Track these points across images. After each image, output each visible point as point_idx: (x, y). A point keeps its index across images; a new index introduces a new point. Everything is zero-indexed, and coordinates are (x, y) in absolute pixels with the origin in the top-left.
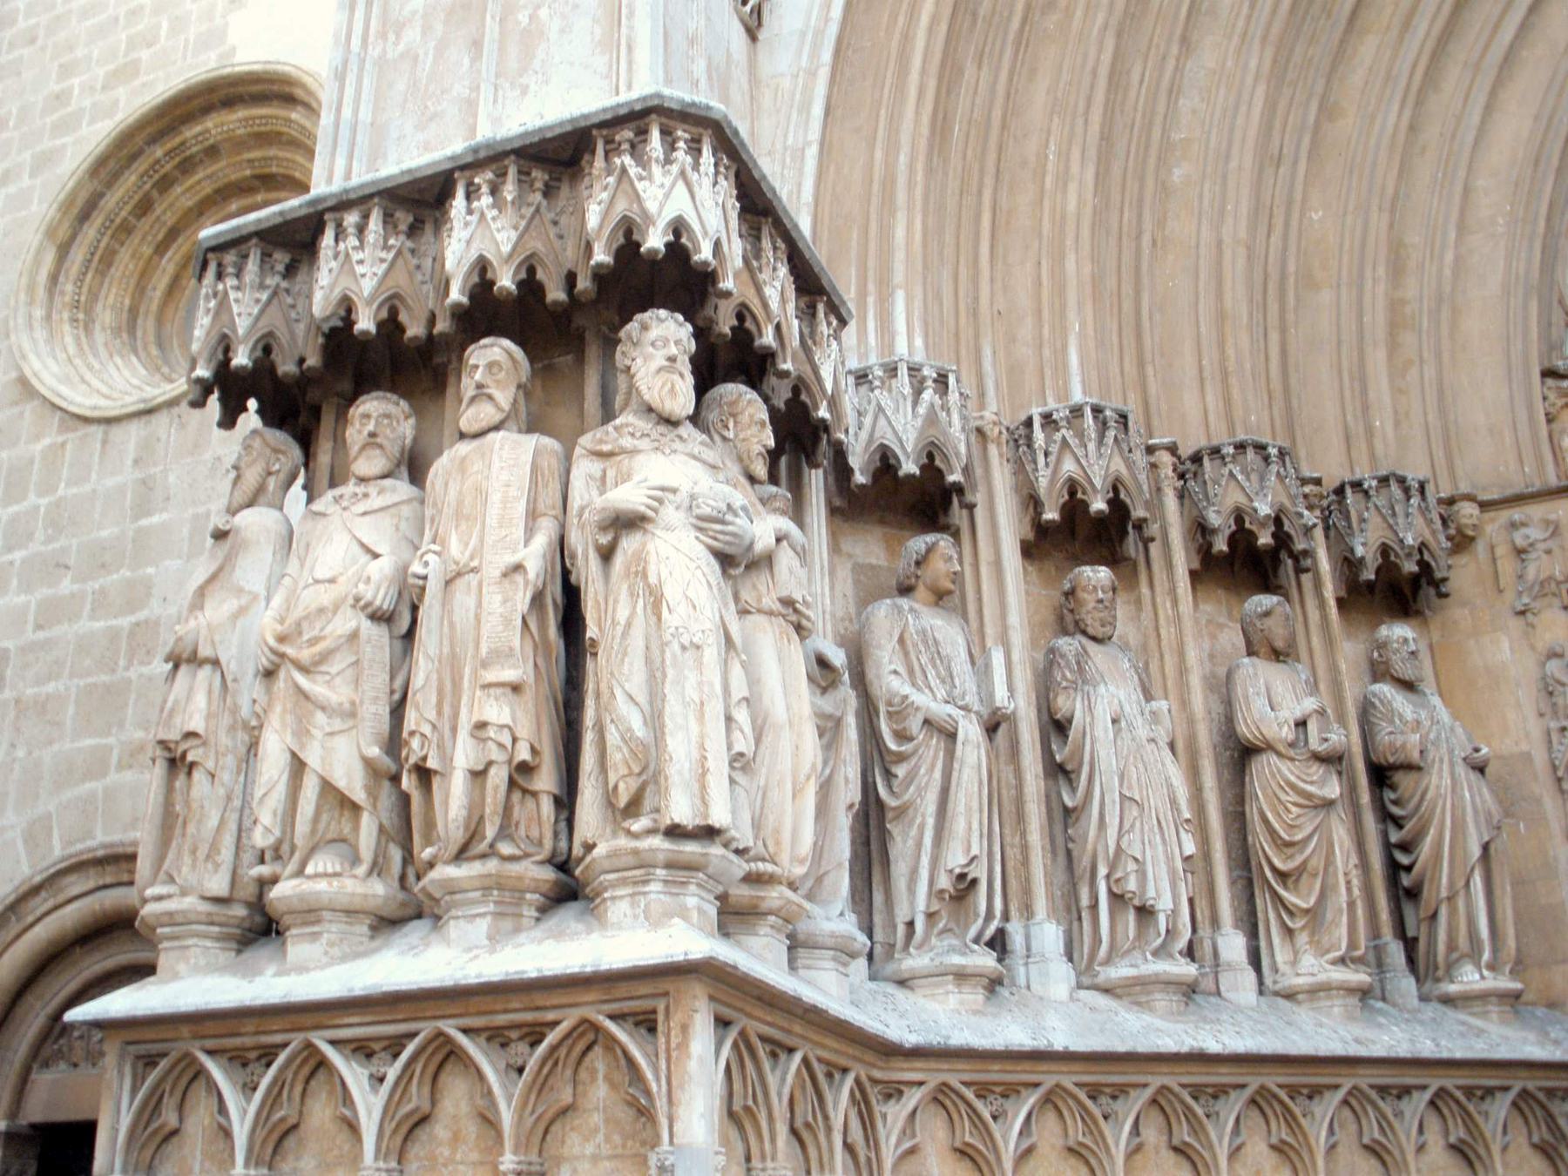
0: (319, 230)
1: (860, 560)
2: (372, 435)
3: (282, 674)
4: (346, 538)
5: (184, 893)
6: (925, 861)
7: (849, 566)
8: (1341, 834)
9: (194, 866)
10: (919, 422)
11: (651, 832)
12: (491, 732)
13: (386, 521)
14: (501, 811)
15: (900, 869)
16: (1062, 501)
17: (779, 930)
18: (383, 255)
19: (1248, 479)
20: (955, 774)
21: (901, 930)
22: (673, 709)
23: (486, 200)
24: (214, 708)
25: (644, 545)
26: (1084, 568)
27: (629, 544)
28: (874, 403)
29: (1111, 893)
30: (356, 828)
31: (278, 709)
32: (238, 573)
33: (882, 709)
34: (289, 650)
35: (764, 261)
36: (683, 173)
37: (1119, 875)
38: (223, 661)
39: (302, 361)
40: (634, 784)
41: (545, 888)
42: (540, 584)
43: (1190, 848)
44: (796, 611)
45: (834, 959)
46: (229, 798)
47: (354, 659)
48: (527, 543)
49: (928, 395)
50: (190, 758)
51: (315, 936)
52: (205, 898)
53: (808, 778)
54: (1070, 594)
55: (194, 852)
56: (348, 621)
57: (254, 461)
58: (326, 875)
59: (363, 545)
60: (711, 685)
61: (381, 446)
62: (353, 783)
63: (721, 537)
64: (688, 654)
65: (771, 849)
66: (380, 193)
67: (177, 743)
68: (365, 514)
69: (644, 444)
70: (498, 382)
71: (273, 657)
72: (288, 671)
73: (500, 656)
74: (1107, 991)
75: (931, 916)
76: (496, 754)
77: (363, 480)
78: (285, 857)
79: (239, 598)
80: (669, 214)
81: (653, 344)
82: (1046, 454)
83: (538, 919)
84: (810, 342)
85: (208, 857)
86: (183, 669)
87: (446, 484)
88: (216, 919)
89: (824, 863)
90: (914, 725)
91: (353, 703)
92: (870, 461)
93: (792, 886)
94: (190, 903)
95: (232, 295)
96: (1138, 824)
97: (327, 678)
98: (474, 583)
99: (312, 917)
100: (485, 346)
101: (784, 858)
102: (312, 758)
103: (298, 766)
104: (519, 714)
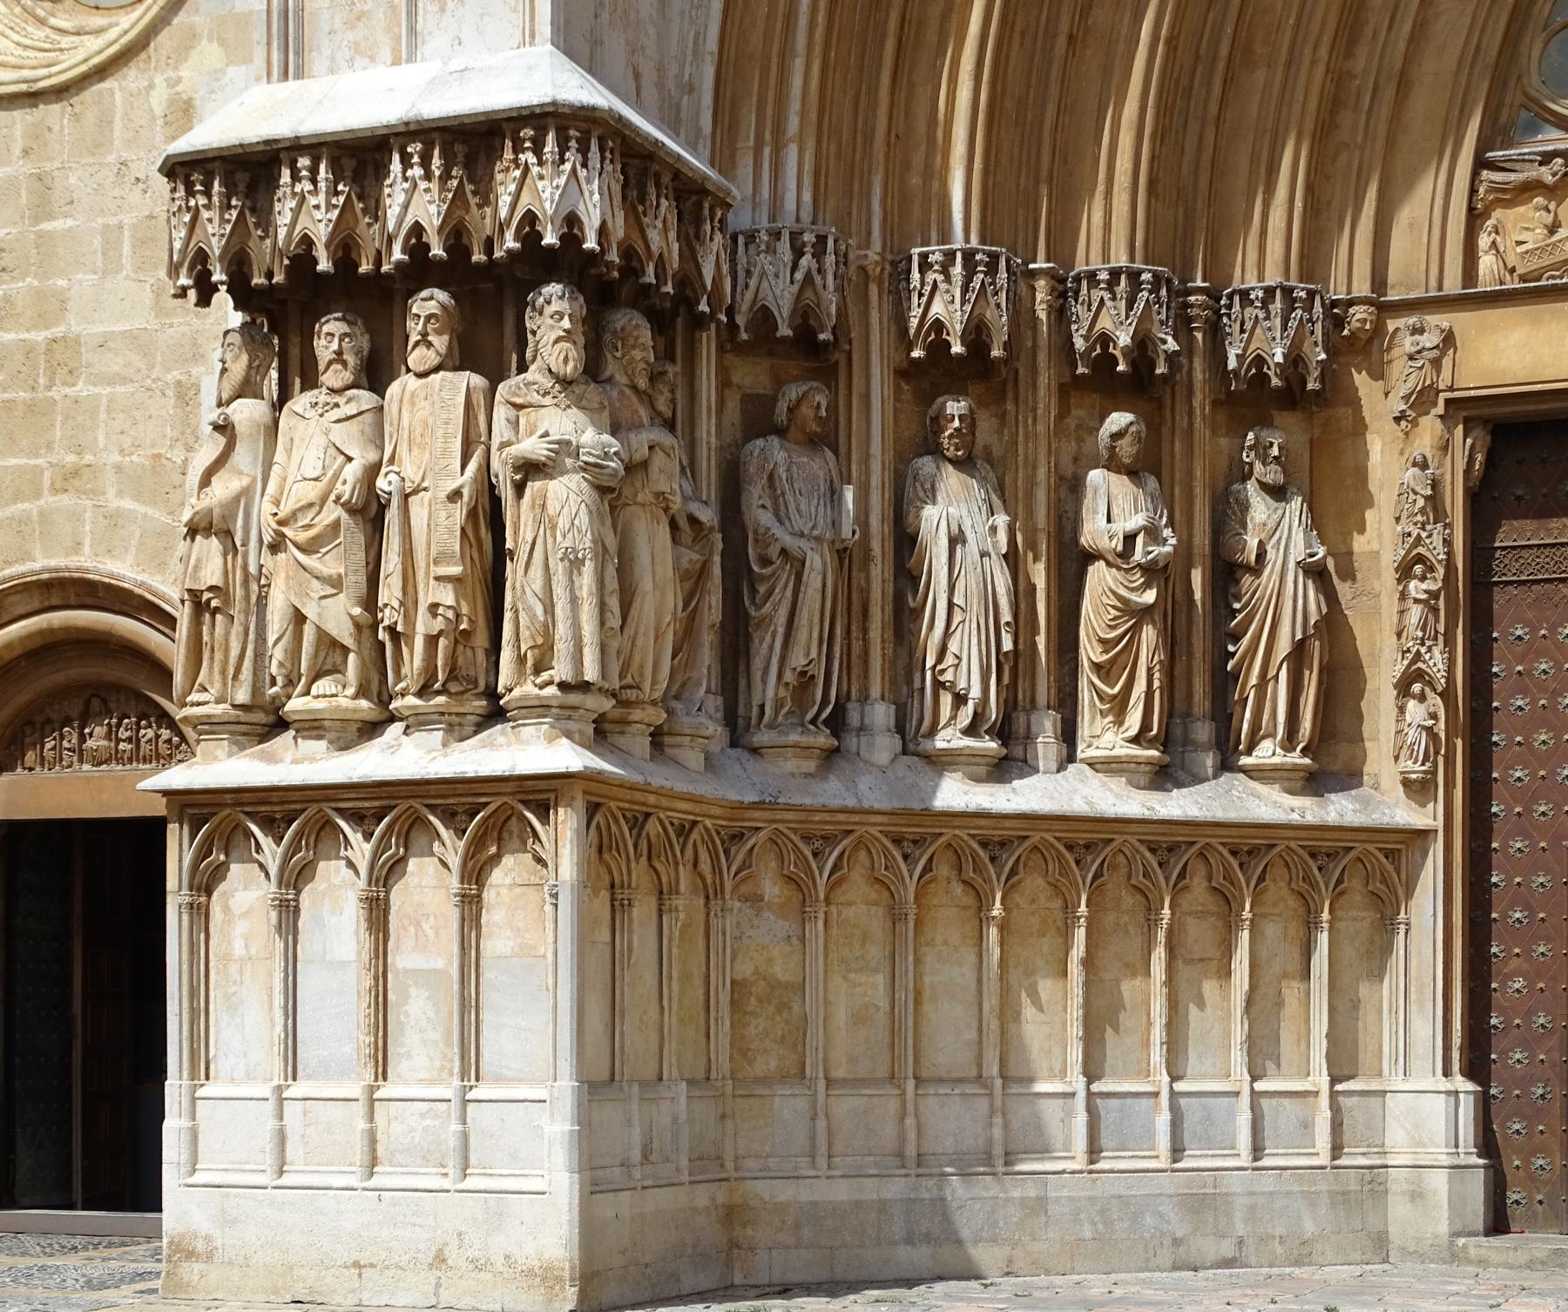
1: (748, 391)
7: (738, 397)
8: (1149, 634)
10: (795, 288)
12: (441, 611)
15: (757, 664)
20: (801, 595)
21: (755, 711)
29: (934, 678)
35: (648, 203)
43: (1007, 645)
49: (806, 261)
58: (325, 696)
62: (343, 631)
69: (548, 400)
75: (779, 704)
78: (295, 681)
82: (921, 295)
90: (773, 552)
102: (310, 611)
103: (299, 618)
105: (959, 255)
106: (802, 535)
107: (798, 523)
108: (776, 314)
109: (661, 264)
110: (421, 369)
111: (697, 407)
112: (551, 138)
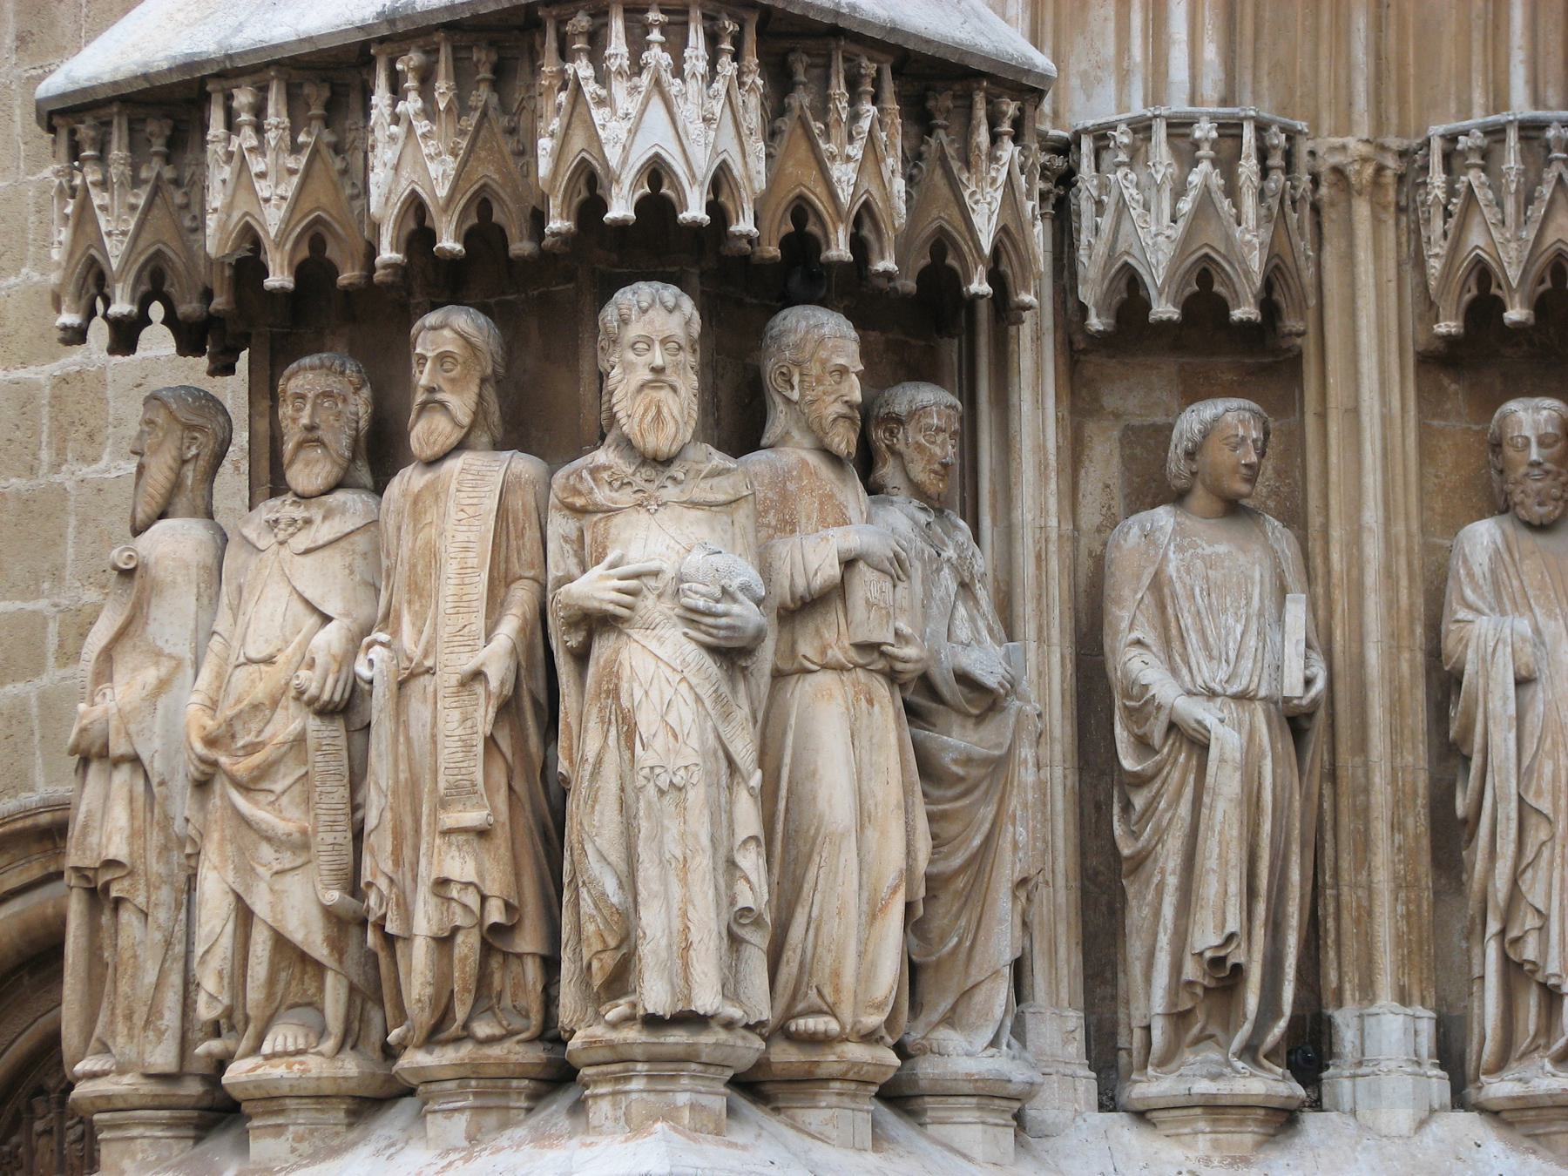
0: (206, 98)
1: (1136, 422)
2: (311, 428)
3: (217, 787)
4: (285, 591)
5: (122, 1071)
6: (1164, 940)
7: (1116, 434)
9: (131, 1037)
10: (1178, 231)
11: (628, 1019)
13: (335, 561)
14: (473, 987)
15: (1135, 948)
16: (1467, 297)
17: (854, 1096)
18: (291, 162)
20: (1205, 811)
21: (1138, 1034)
22: (648, 871)
23: (412, 104)
24: (137, 824)
25: (617, 652)
26: (1512, 405)
27: (603, 649)
28: (1115, 193)
30: (321, 989)
31: (216, 836)
32: (152, 628)
33: (1118, 703)
34: (224, 760)
35: (832, 117)
36: (657, 83)
37: (1514, 933)
38: (145, 757)
39: (208, 295)
40: (610, 959)
41: (535, 1072)
42: (508, 690)
44: (883, 654)
45: (980, 1108)
46: (168, 944)
47: (303, 771)
48: (489, 637)
51: (279, 1130)
53: (895, 891)
54: (1497, 446)
55: (129, 1017)
56: (289, 722)
57: (160, 444)
58: (286, 1054)
59: (307, 603)
60: (696, 837)
62: (310, 935)
63: (714, 631)
64: (667, 800)
65: (830, 999)
66: (277, 63)
67: (96, 869)
68: (307, 552)
69: (625, 497)
70: (453, 381)
71: (203, 767)
72: (223, 786)
73: (460, 793)
74: (1494, 1114)
75: (1179, 1019)
77: (303, 497)
78: (240, 1026)
79: (157, 664)
80: (639, 157)
81: (633, 346)
82: (1448, 214)
83: (529, 1110)
84: (956, 165)
85: (148, 1022)
86: (94, 768)
87: (399, 529)
89: (974, 971)
90: (1157, 731)
92: (1110, 291)
93: (869, 1038)
95: (98, 197)
96: (1546, 853)
97: (272, 798)
98: (430, 689)
99: (274, 1105)
101: (846, 1012)
102: (261, 905)
104: (488, 864)
105: (1512, 136)
106: (1212, 694)
107: (1209, 673)
108: (1147, 279)
109: (865, 216)
110: (428, 453)
111: (1014, 465)
112: (617, 26)
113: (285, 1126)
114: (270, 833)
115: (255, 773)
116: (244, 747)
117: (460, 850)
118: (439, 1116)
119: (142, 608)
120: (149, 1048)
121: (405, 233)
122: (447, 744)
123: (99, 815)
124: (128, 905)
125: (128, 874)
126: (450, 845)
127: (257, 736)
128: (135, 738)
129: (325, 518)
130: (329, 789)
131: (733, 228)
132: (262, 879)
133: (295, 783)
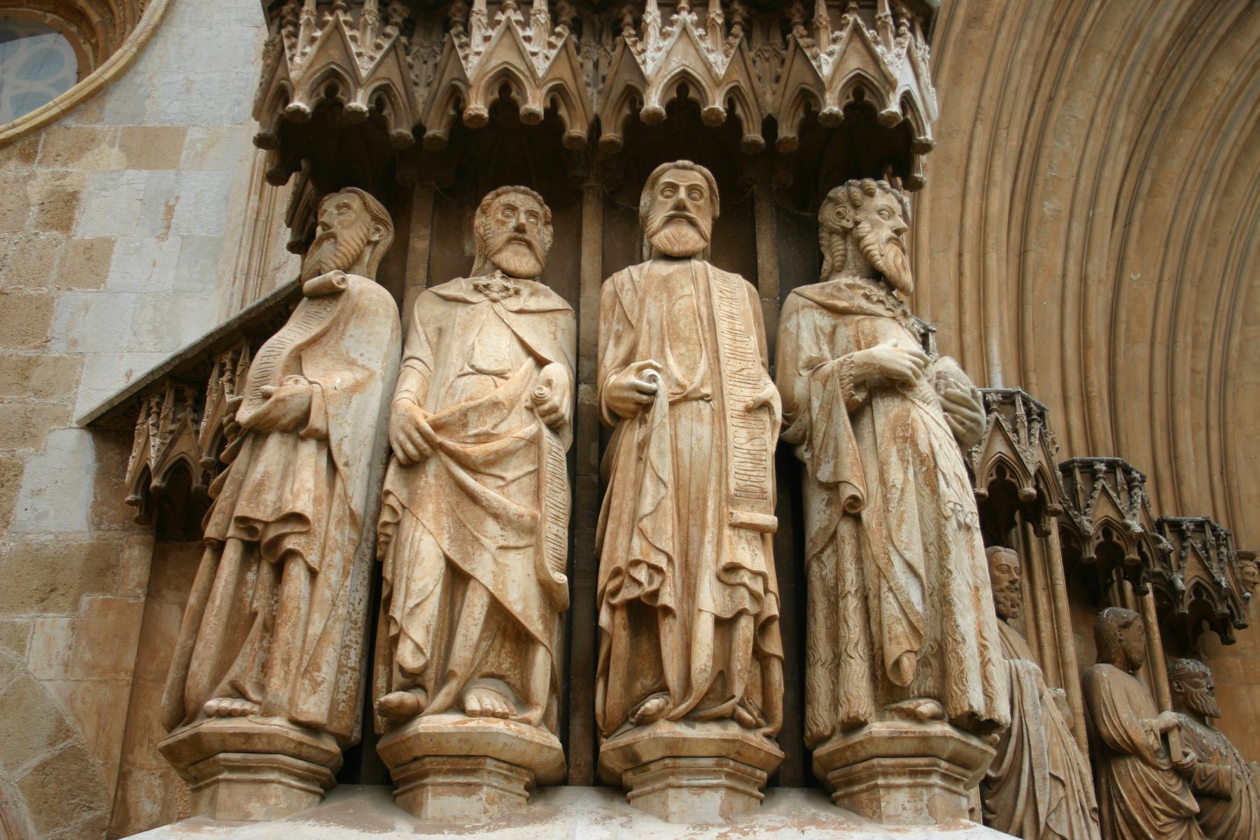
3: (432, 468)
5: (268, 712)
19: (1118, 496)
31: (431, 507)
47: (531, 468)
50: (290, 544)
51: (470, 789)
52: (295, 722)
55: (287, 662)
56: (521, 426)
61: (529, 245)
67: (266, 524)
69: (879, 309)
73: (747, 496)
76: (747, 604)
77: (508, 274)
78: (430, 685)
81: (879, 212)
85: (306, 670)
88: (304, 750)
91: (534, 518)
94: (277, 724)
97: (501, 483)
99: (468, 764)
100: (684, 168)
113: (479, 786)
114: (500, 511)
115: (491, 457)
116: (476, 435)
117: (749, 544)
118: (685, 792)
119: (338, 326)
120: (303, 695)
121: (668, 98)
122: (737, 454)
123: (277, 478)
124: (300, 561)
125: (306, 533)
126: (740, 537)
127: (493, 429)
128: (330, 419)
129: (532, 294)
130: (556, 489)
131: (916, 175)
132: (486, 549)
133: (524, 476)
